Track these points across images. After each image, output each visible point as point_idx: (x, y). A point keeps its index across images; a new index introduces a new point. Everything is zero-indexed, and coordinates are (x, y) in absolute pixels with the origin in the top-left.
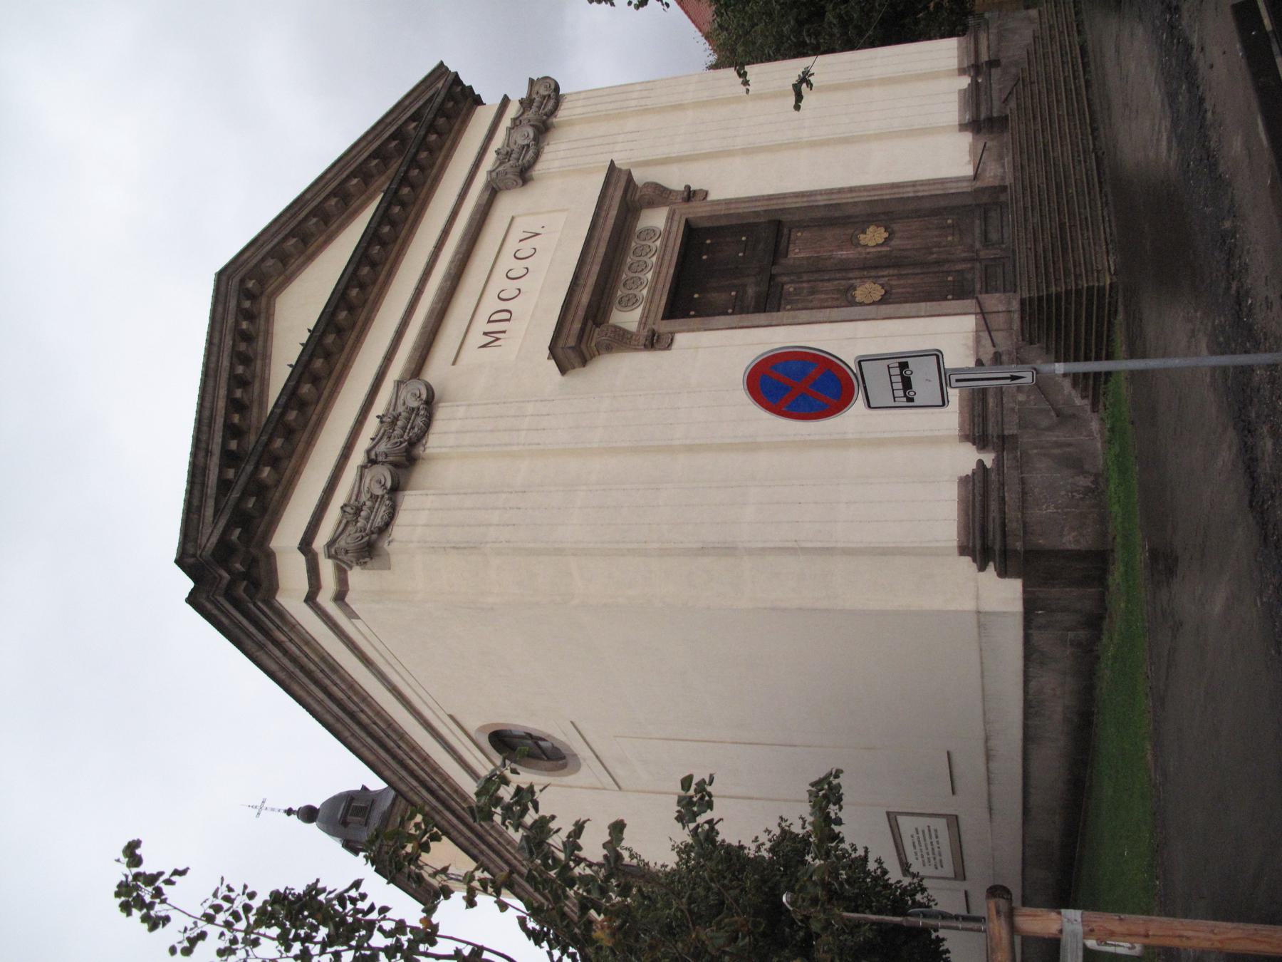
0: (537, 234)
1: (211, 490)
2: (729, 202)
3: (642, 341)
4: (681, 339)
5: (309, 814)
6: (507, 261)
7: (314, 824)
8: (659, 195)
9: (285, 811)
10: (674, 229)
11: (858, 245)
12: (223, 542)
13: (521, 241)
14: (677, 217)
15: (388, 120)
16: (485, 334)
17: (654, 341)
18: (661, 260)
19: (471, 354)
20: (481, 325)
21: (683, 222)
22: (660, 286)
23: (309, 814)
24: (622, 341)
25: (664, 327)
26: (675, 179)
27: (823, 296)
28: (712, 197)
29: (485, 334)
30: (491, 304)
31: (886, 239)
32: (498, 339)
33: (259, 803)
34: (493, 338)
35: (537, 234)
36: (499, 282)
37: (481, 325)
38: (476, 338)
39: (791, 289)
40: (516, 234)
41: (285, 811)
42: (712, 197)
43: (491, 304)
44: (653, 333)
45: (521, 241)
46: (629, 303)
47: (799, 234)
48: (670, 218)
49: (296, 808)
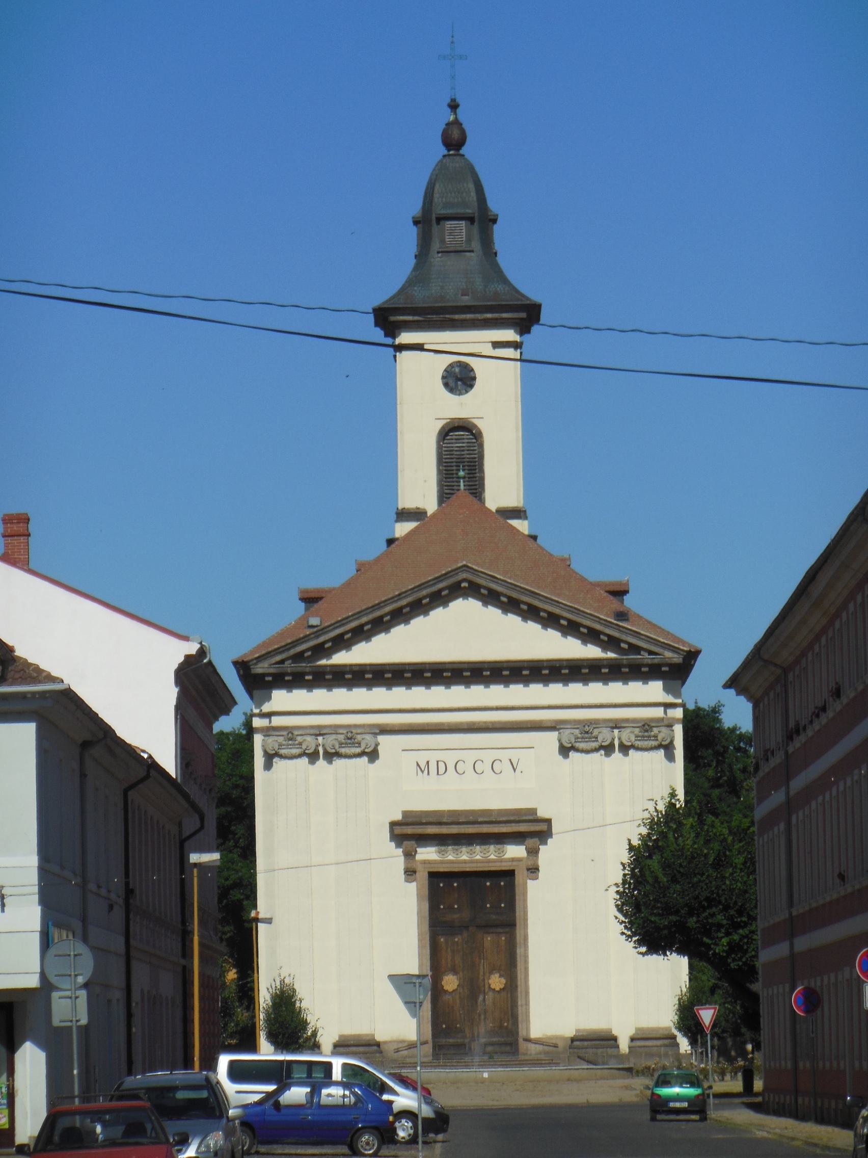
0: (515, 770)
11: (491, 973)
12: (264, 675)
13: (510, 760)
14: (515, 863)
18: (477, 861)
20: (433, 757)
21: (511, 868)
27: (449, 958)
29: (428, 762)
31: (494, 989)
32: (422, 772)
35: (515, 770)
38: (422, 758)
39: (456, 940)
40: (514, 755)
43: (450, 758)
45: (510, 760)
47: (503, 938)
48: (513, 860)
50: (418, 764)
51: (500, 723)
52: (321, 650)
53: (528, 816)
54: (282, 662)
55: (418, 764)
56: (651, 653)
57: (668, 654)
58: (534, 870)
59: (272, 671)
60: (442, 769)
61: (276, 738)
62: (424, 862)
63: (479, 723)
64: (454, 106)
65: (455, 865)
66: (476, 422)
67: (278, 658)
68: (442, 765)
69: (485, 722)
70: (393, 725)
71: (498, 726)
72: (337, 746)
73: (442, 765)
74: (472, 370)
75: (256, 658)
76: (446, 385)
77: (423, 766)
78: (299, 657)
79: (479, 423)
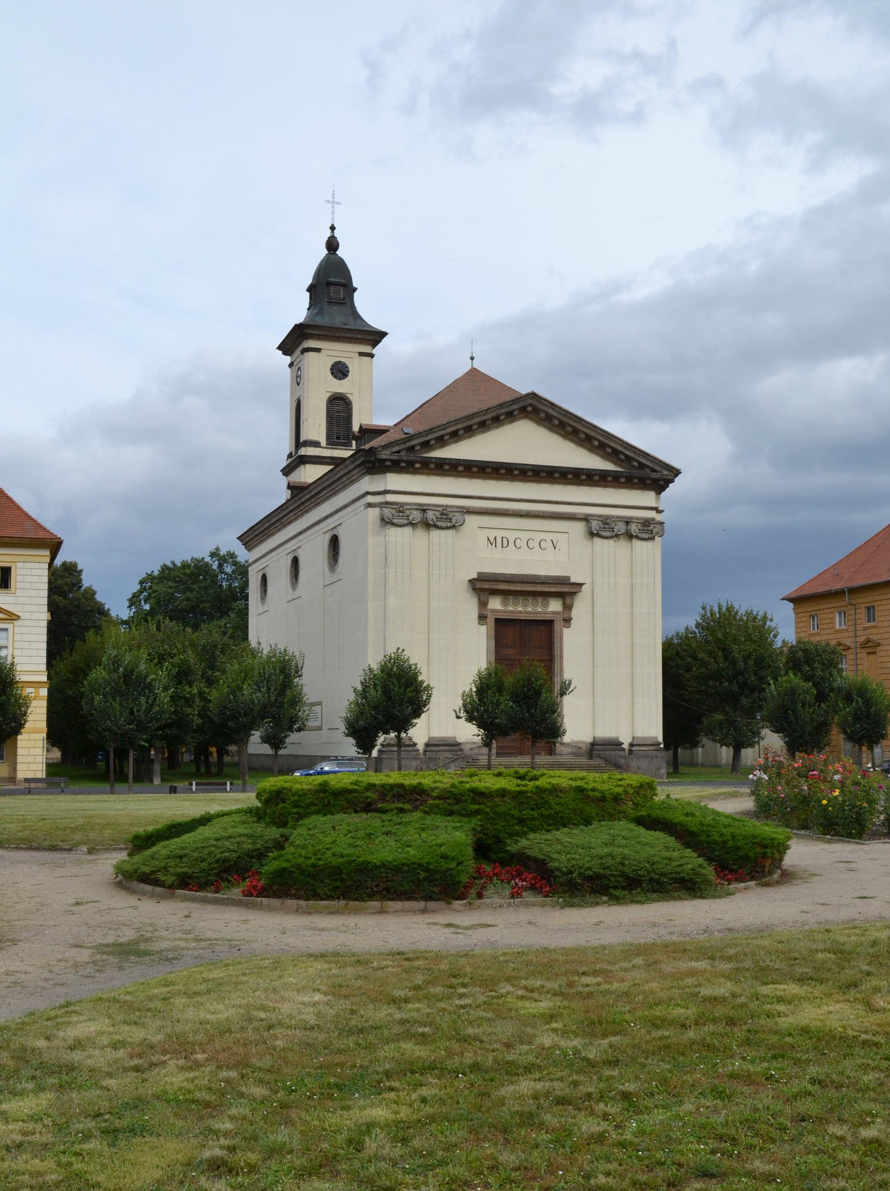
0: (555, 548)
1: (408, 445)
2: (561, 638)
3: (483, 613)
4: (484, 628)
5: (332, 245)
6: (538, 537)
7: (326, 252)
8: (568, 607)
9: (333, 225)
10: (547, 615)
12: (384, 460)
14: (555, 615)
15: (637, 451)
16: (495, 538)
17: (482, 618)
18: (529, 613)
19: (483, 535)
20: (499, 534)
22: (514, 614)
23: (332, 245)
24: (483, 604)
25: (491, 621)
26: (575, 613)
28: (565, 630)
29: (495, 538)
30: (511, 535)
33: (336, 200)
34: (493, 542)
36: (525, 536)
37: (499, 534)
38: (492, 534)
41: (333, 225)
42: (565, 630)
43: (511, 535)
44: (486, 617)
46: (505, 603)
48: (554, 613)
49: (337, 233)
50: (488, 539)
51: (548, 512)
52: (426, 446)
53: (563, 581)
54: (398, 452)
55: (488, 539)
56: (653, 470)
57: (665, 472)
58: (568, 621)
59: (392, 457)
60: (505, 543)
61: (390, 510)
62: (493, 611)
63: (533, 511)
64: (333, 228)
65: (514, 614)
66: (349, 396)
67: (397, 448)
68: (505, 541)
69: (538, 511)
70: (474, 508)
71: (546, 515)
72: (435, 520)
73: (504, 540)
74: (347, 367)
75: (383, 446)
76: (332, 374)
77: (492, 540)
78: (411, 449)
79: (350, 396)
